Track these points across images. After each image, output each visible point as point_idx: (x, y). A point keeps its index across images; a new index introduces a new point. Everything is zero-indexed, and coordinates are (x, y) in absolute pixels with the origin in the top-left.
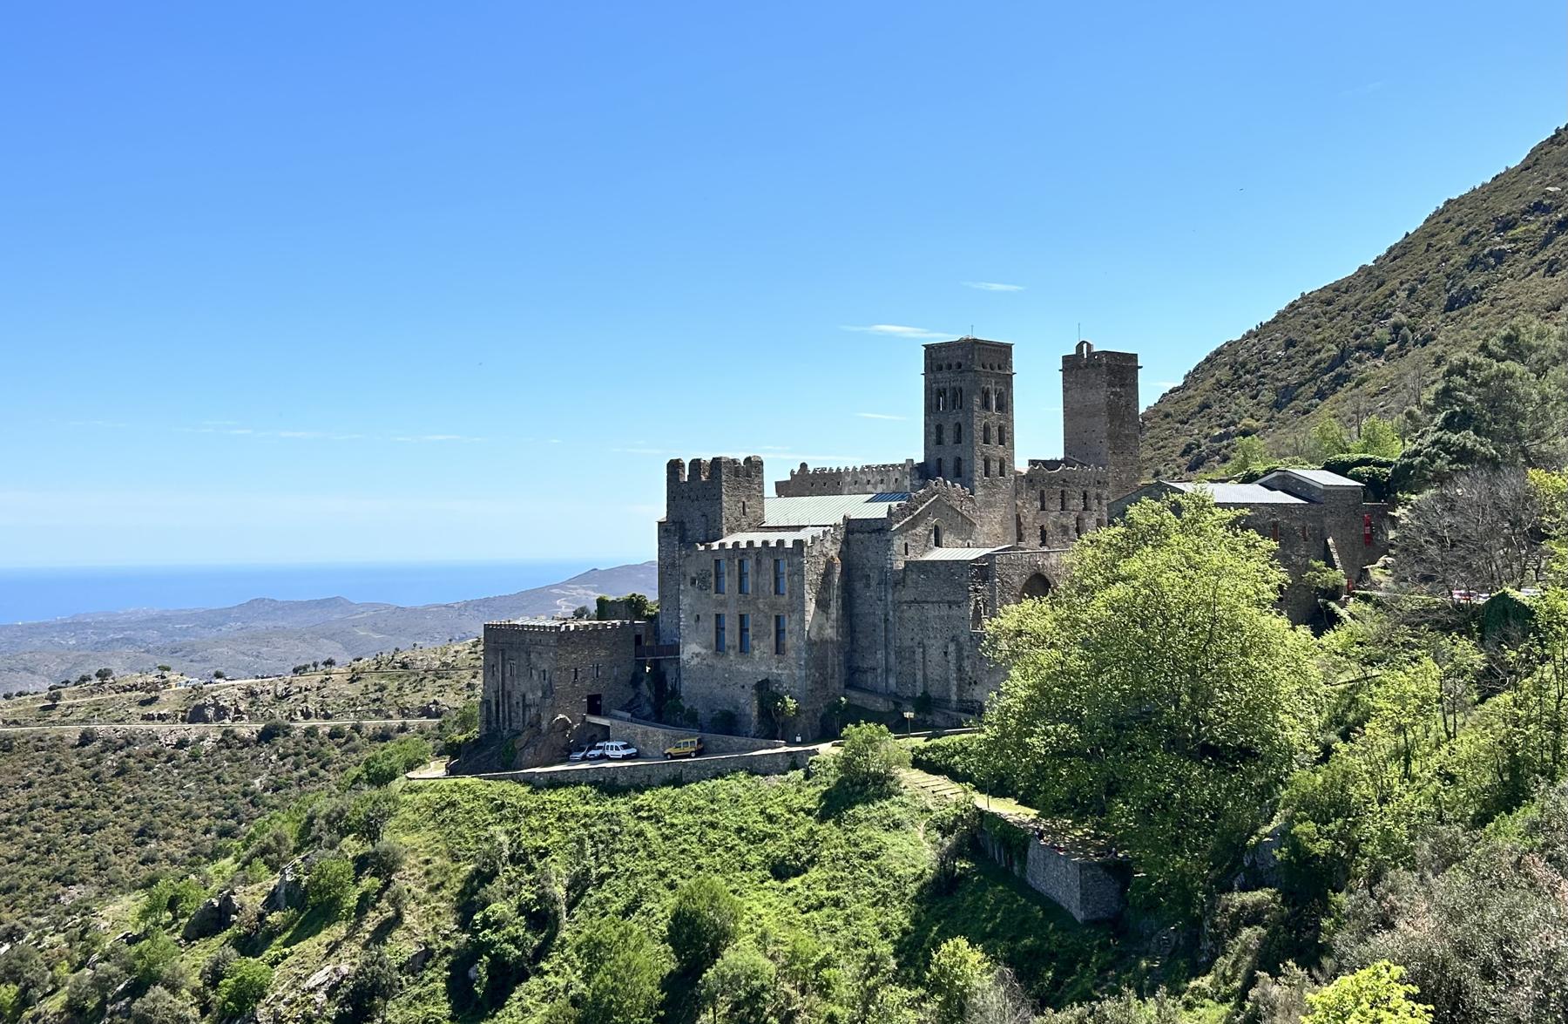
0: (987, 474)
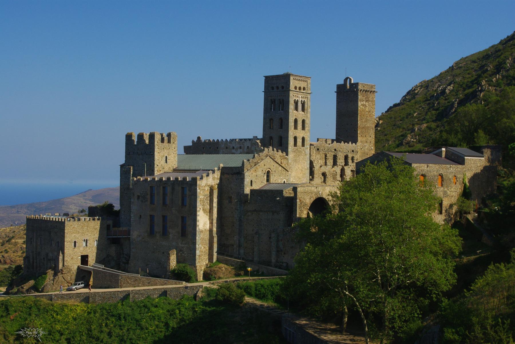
0: (295, 144)
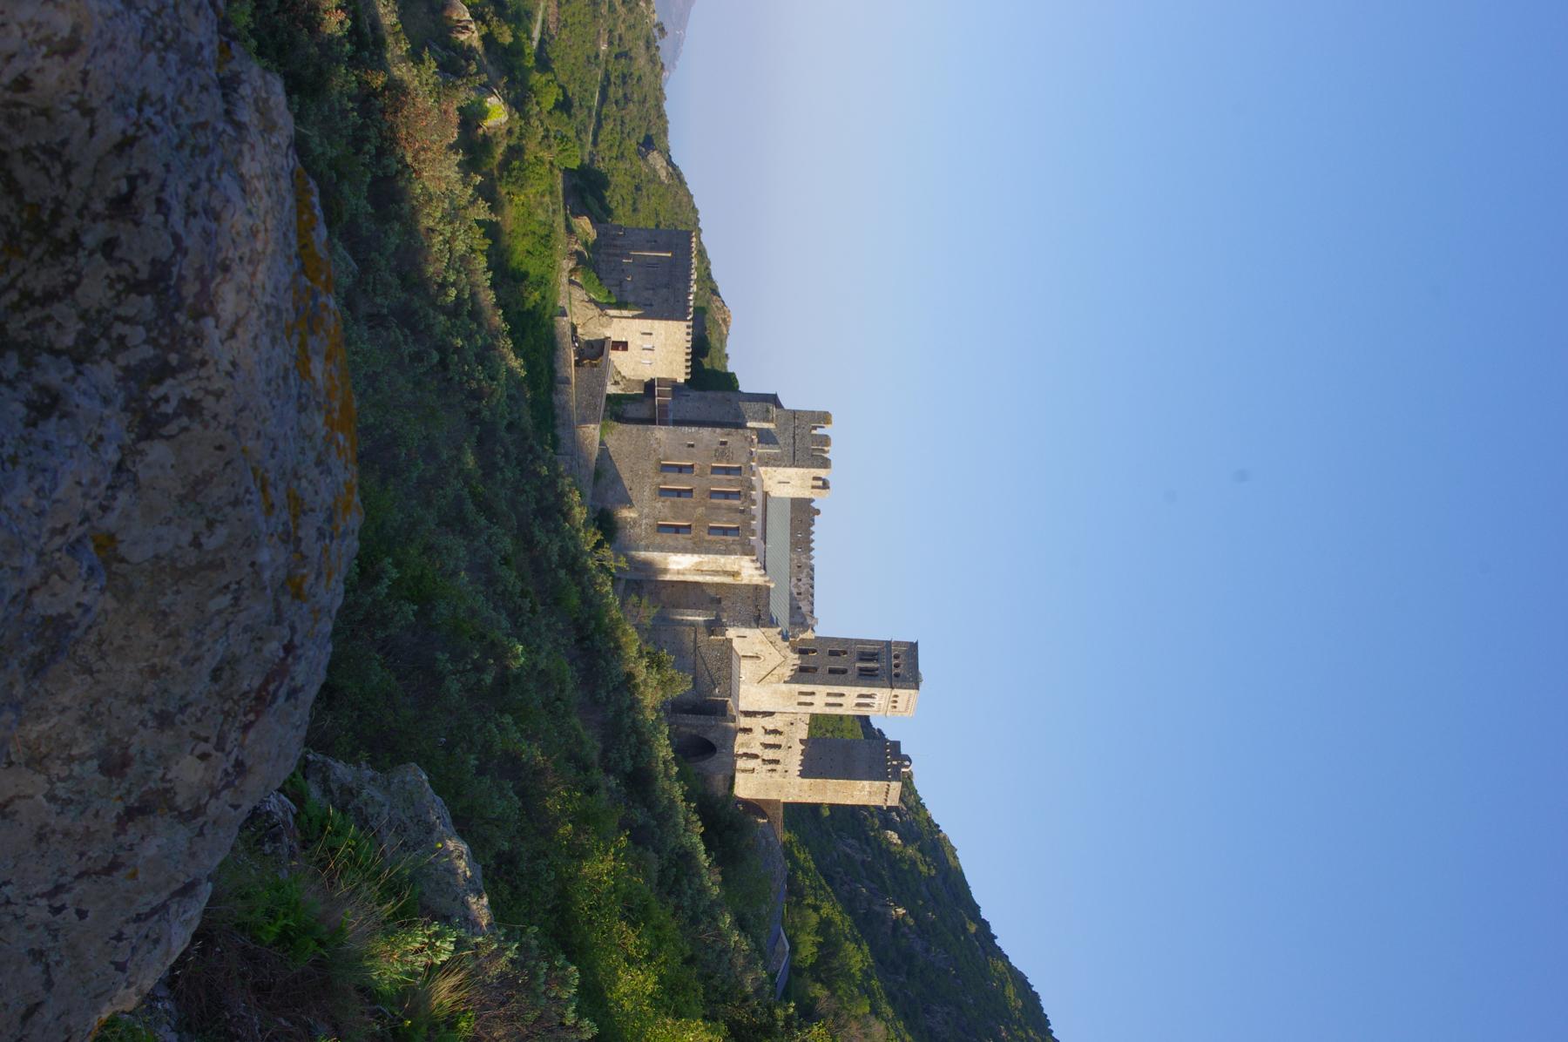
0: (801, 693)
